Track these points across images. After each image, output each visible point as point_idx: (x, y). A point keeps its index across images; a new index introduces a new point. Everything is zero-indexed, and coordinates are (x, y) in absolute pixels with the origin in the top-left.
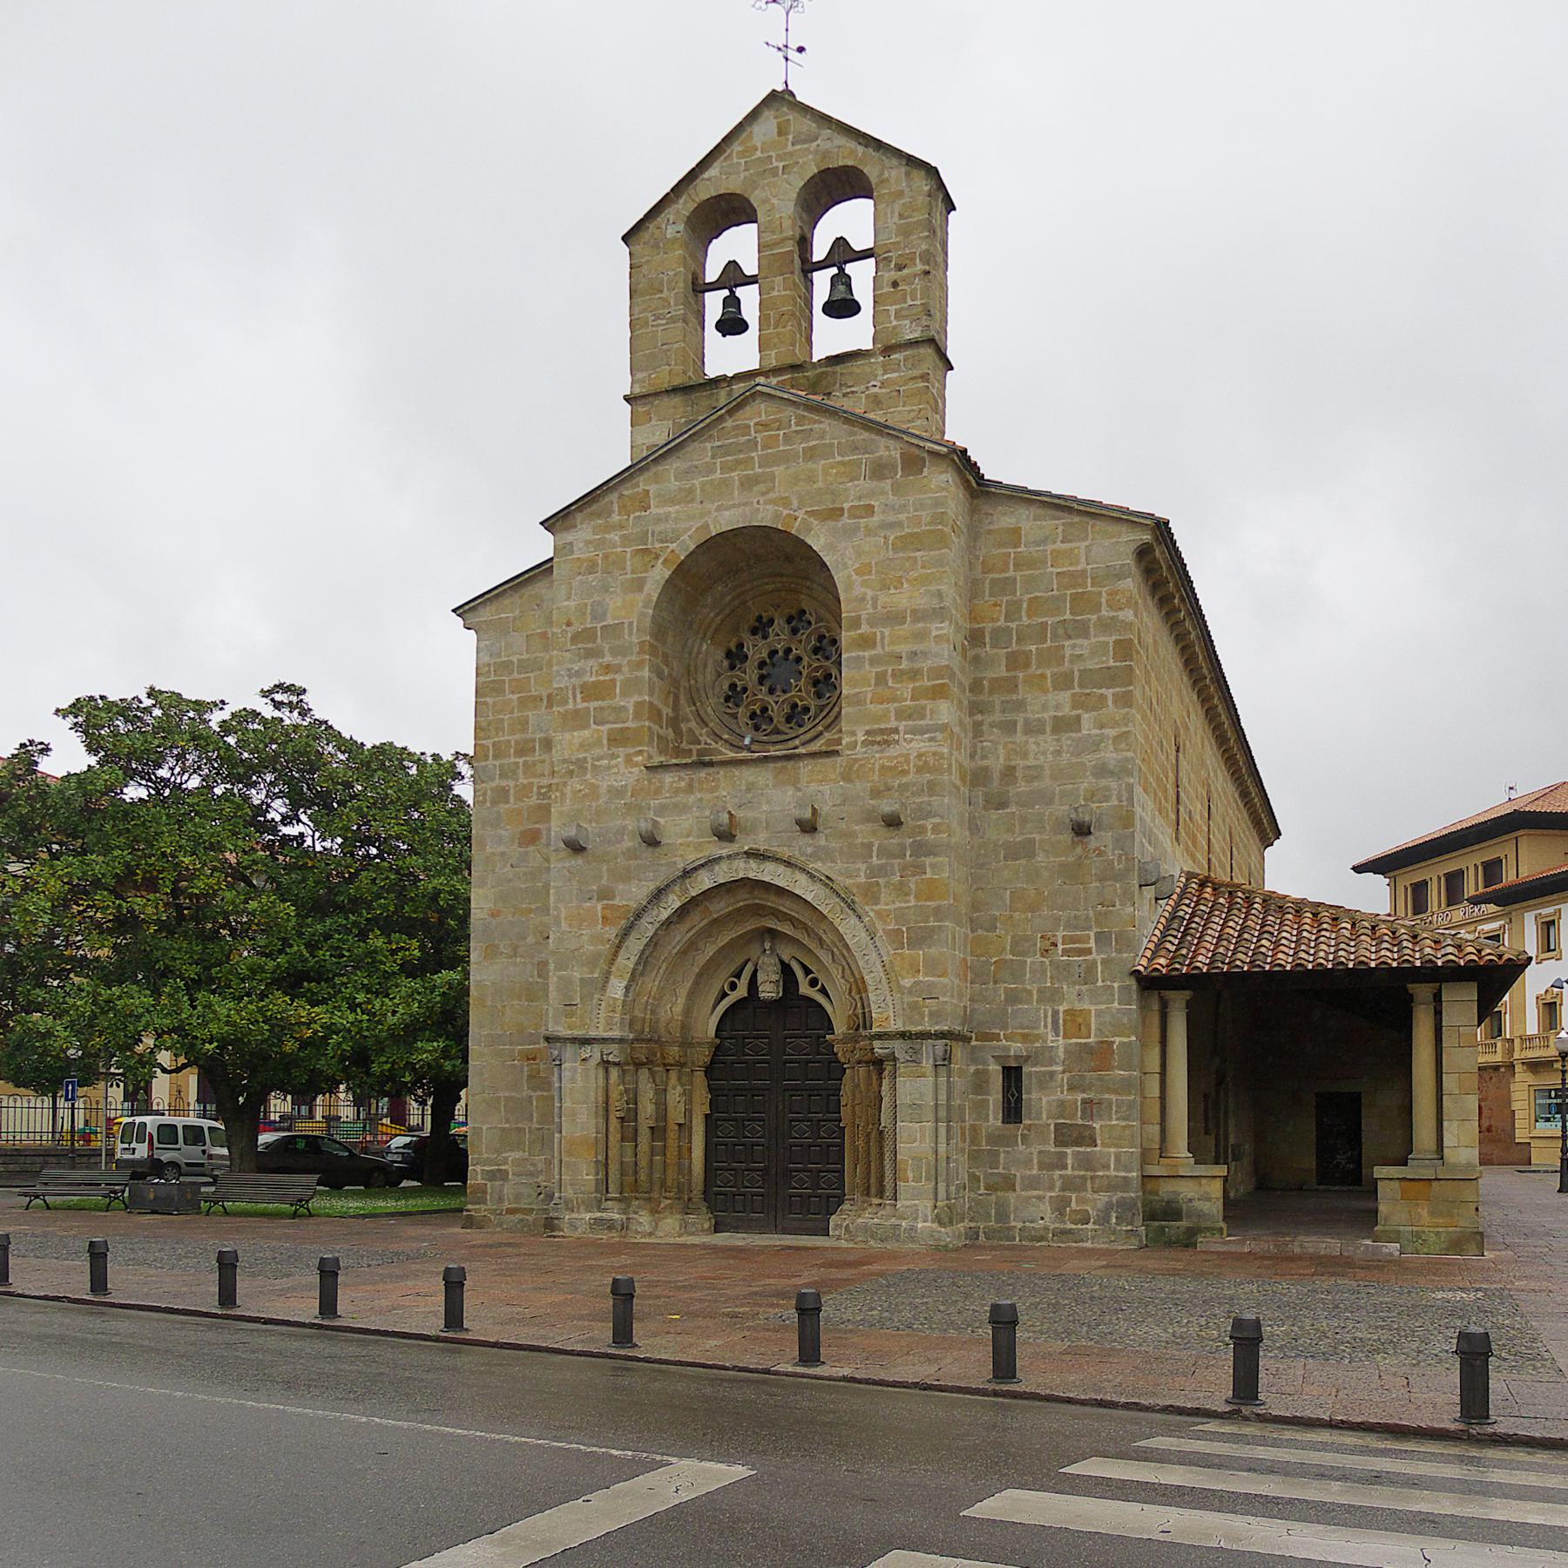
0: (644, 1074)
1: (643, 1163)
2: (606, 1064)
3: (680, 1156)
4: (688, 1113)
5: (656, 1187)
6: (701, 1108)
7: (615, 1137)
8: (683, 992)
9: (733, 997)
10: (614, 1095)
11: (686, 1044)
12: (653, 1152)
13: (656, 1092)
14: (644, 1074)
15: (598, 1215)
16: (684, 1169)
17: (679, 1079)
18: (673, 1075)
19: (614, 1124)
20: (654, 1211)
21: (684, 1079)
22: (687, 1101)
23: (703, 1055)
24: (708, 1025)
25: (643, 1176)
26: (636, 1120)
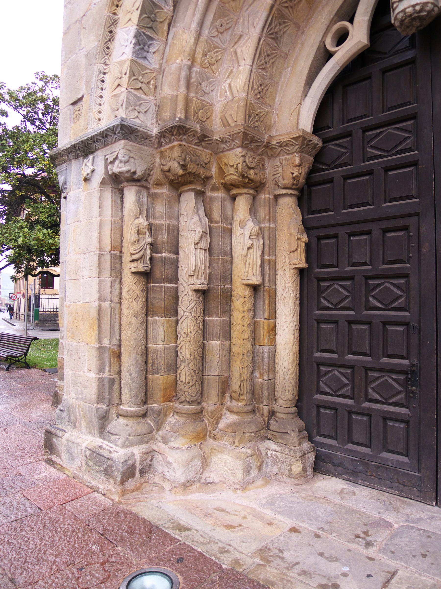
0: (189, 200)
1: (186, 351)
2: (116, 182)
3: (254, 339)
4: (268, 266)
5: (213, 392)
6: (290, 256)
7: (132, 306)
8: (247, 49)
9: (343, 54)
10: (130, 235)
11: (253, 139)
12: (205, 332)
13: (210, 232)
14: (189, 200)
15: (97, 441)
16: (260, 360)
17: (253, 210)
18: (242, 204)
19: (131, 285)
20: (201, 437)
21: (262, 212)
22: (266, 246)
23: (288, 168)
24: (296, 111)
25: (185, 374)
26: (175, 279)
